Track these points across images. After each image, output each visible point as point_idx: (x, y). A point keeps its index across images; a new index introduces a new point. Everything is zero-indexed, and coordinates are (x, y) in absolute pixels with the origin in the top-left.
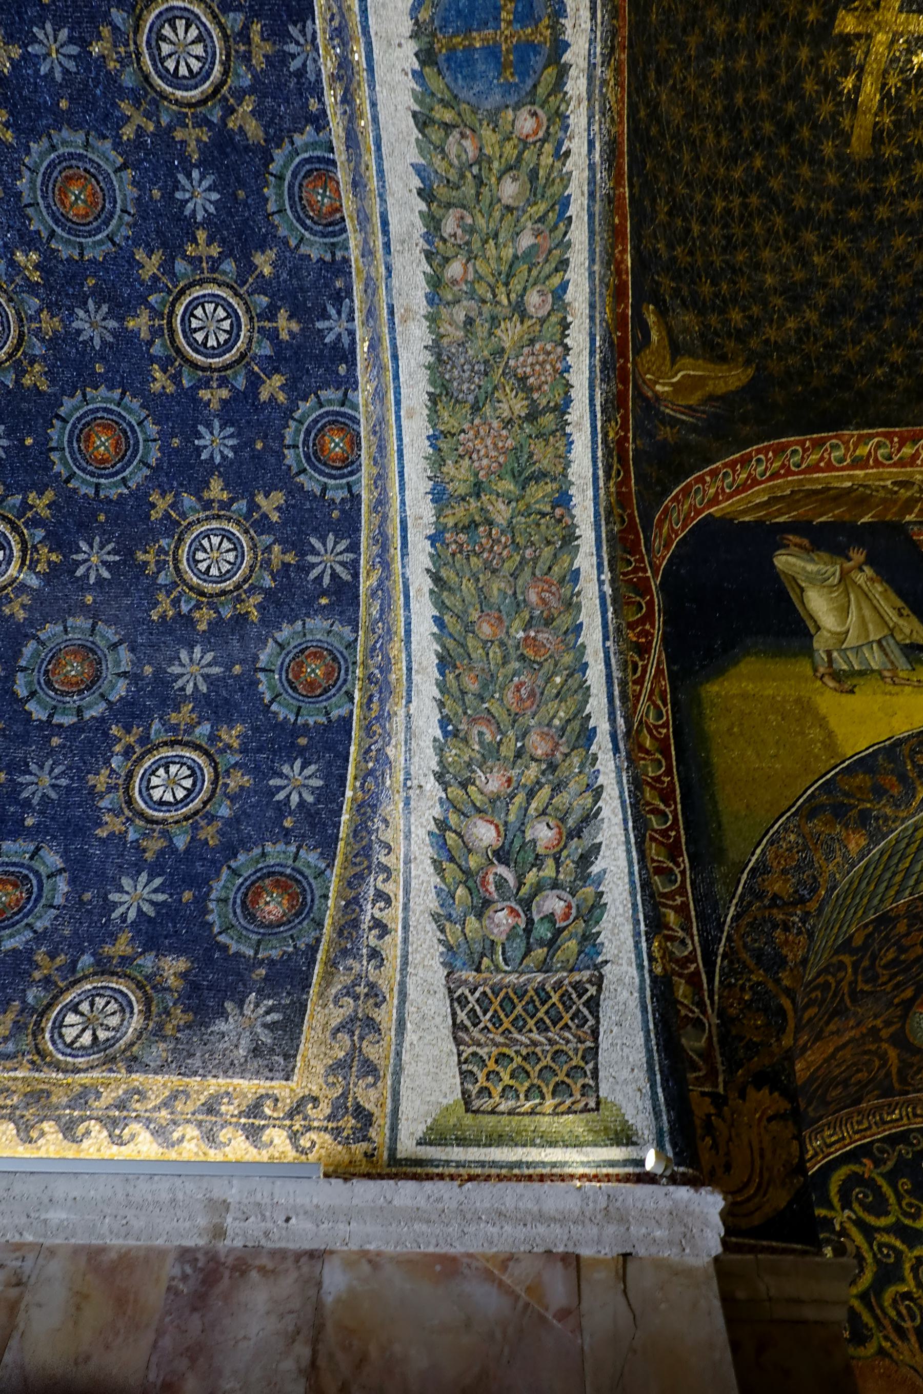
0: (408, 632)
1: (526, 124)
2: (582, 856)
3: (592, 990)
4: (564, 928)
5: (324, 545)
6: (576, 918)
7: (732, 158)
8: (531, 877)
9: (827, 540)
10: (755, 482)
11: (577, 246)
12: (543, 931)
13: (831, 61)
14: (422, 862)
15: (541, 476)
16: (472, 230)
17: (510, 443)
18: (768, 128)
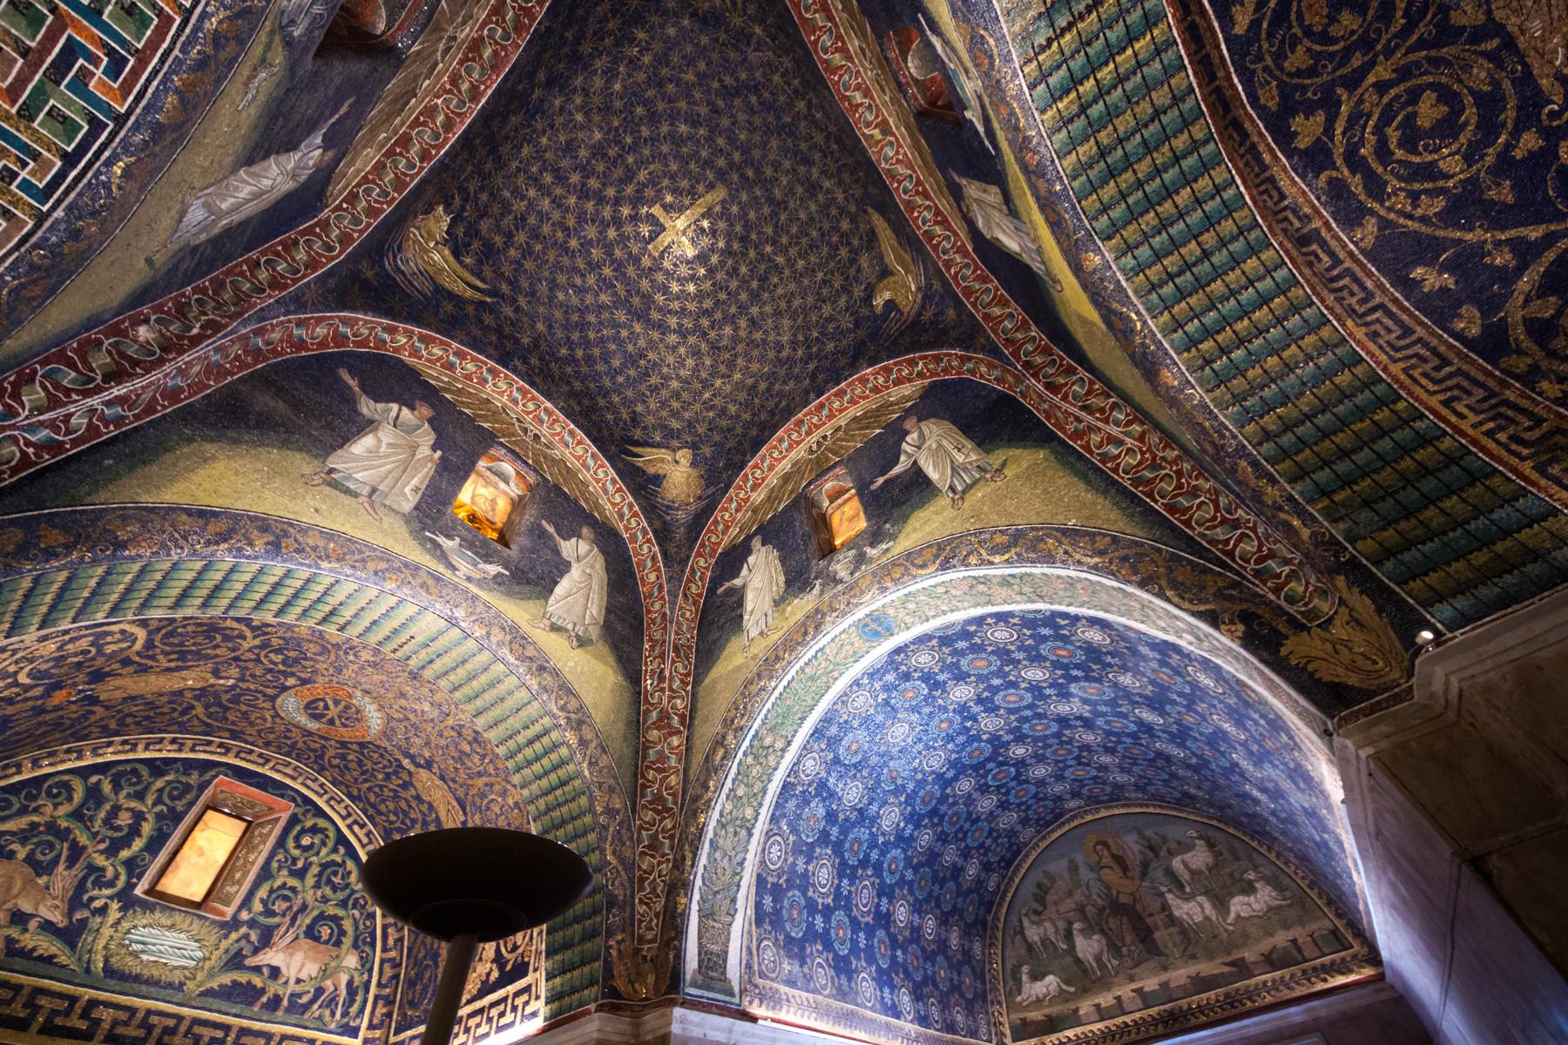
1: (891, 612)
7: (778, 269)
10: (938, 213)
13: (706, 241)
18: (752, 254)
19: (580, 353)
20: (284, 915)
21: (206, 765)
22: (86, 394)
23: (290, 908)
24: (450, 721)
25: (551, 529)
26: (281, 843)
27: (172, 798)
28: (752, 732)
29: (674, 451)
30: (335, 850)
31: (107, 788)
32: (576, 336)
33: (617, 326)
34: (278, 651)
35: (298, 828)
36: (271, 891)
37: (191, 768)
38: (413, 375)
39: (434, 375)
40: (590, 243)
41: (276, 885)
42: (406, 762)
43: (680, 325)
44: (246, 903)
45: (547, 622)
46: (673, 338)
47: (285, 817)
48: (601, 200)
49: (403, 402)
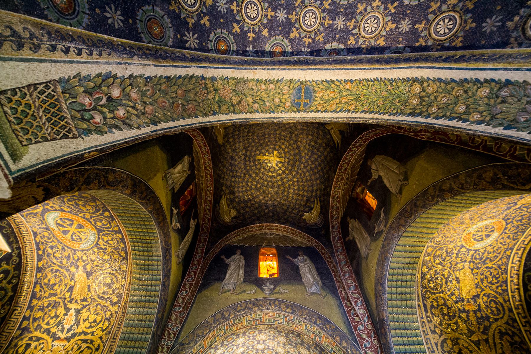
0: (175, 66)
1: (288, 104)
2: (117, 126)
3: (71, 135)
4: (90, 123)
5: (195, 39)
6: (95, 126)
8: (105, 110)
9: (191, 166)
10: (201, 149)
11: (266, 115)
12: (87, 116)
13: (270, 151)
14: (99, 69)
15: (220, 107)
16: (270, 91)
17: (227, 99)
19: (319, 168)
22: (355, 311)
25: (370, 181)
28: (410, 119)
29: (329, 130)
32: (316, 171)
33: (307, 161)
38: (342, 218)
39: (341, 213)
40: (292, 176)
43: (294, 144)
45: (398, 196)
46: (299, 144)
48: (282, 179)
49: (348, 227)
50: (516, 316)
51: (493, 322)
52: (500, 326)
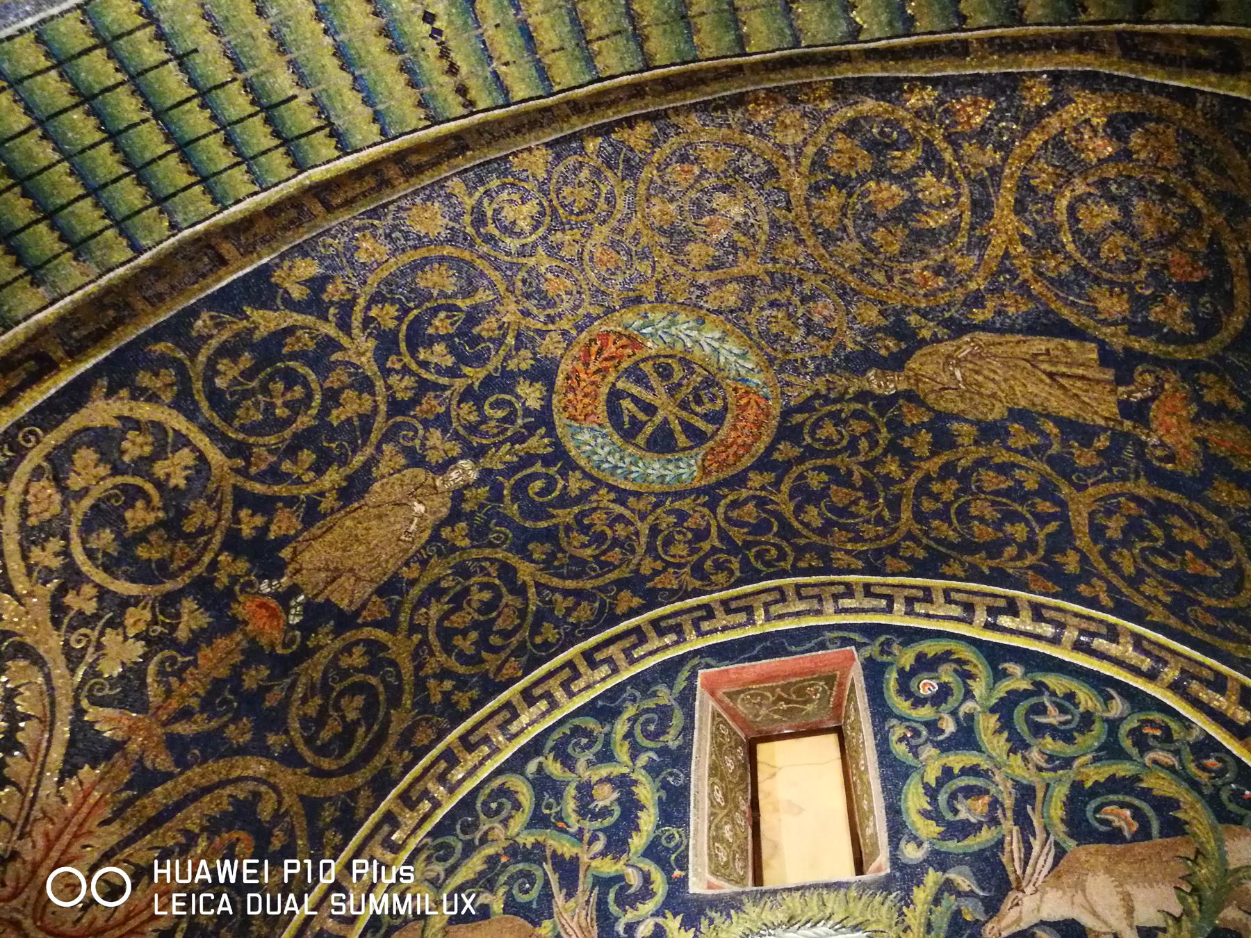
20: (994, 821)
21: (668, 671)
23: (995, 803)
24: (799, 185)
26: (881, 712)
27: (653, 736)
30: (999, 675)
31: (555, 769)
34: (418, 338)
35: (892, 677)
36: (931, 793)
37: (649, 685)
41: (931, 776)
42: (873, 381)
44: (897, 829)
47: (856, 674)
50: (374, 817)
51: (265, 752)
52: (274, 788)
